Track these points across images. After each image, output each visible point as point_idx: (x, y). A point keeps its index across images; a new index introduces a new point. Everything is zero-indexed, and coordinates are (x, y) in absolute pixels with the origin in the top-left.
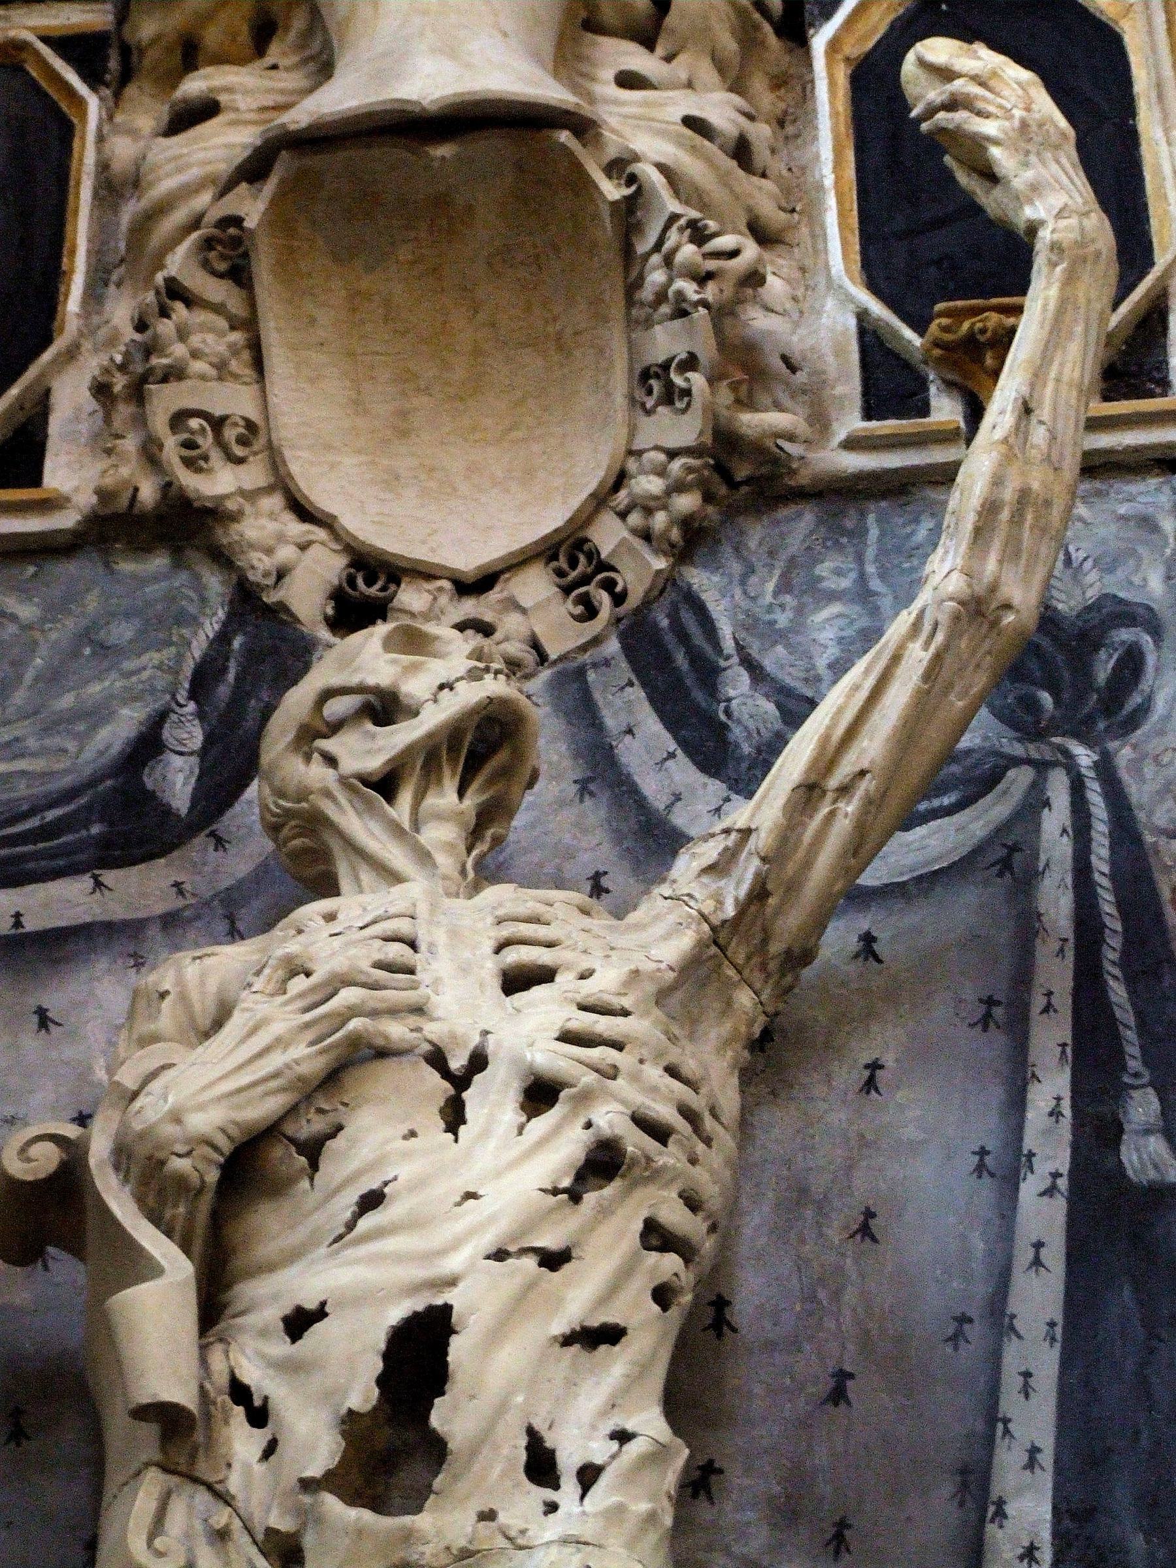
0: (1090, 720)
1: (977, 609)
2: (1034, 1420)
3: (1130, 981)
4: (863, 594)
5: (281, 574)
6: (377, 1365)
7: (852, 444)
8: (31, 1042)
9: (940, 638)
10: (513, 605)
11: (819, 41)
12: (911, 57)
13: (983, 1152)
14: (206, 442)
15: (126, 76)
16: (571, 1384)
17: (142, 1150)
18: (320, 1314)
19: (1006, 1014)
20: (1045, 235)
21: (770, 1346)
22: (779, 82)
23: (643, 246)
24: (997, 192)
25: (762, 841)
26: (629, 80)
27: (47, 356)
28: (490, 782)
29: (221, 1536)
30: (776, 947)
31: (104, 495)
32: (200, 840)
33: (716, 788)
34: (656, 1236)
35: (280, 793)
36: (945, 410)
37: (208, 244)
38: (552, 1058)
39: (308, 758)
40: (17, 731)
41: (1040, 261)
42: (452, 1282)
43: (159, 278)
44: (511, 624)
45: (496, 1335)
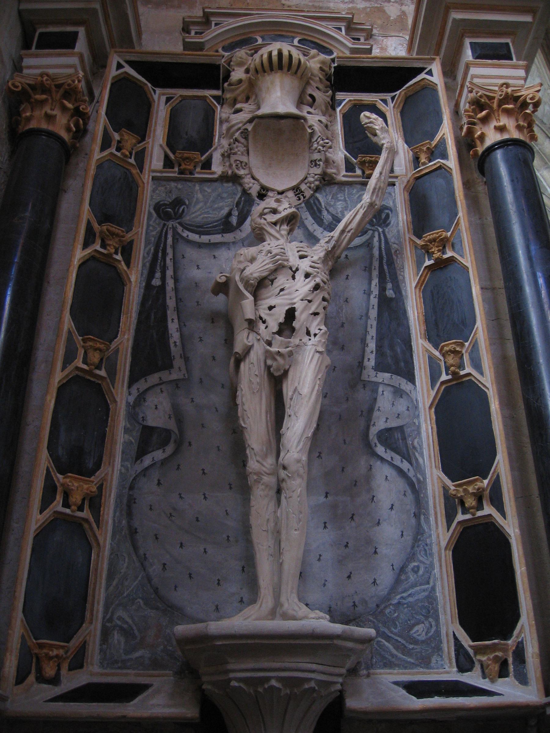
0: (381, 224)
1: (371, 205)
2: (373, 332)
3: (388, 265)
4: (345, 200)
5: (250, 188)
6: (284, 316)
7: (344, 176)
8: (213, 261)
9: (365, 209)
10: (286, 197)
11: (338, 110)
12: (362, 114)
13: (365, 290)
14: (239, 165)
16: (312, 321)
17: (246, 279)
18: (274, 307)
19: (368, 269)
20: (385, 146)
21: (332, 318)
22: (330, 116)
23: (313, 141)
24: (376, 138)
25: (335, 238)
28: (292, 225)
29: (259, 340)
30: (336, 256)
31: (223, 172)
32: (238, 230)
33: (321, 229)
34: (324, 299)
35: (256, 224)
36: (359, 172)
37: (242, 133)
38: (310, 270)
39: (261, 219)
41: (384, 150)
42: (295, 304)
43: (234, 137)
45: (302, 312)
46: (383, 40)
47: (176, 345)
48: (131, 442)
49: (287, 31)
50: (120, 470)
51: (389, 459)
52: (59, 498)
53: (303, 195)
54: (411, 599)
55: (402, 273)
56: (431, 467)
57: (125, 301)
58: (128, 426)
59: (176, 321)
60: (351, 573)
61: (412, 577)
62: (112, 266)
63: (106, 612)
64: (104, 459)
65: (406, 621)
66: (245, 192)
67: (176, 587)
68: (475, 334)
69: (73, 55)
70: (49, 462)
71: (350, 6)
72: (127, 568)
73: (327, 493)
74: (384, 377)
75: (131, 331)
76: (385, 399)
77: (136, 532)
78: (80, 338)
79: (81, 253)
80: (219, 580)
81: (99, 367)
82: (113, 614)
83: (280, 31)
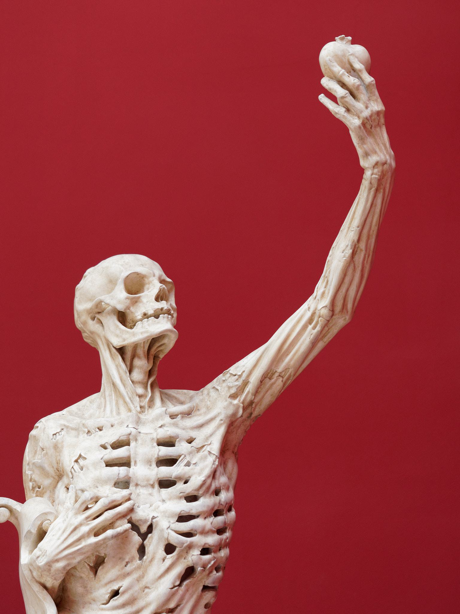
9: (318, 328)
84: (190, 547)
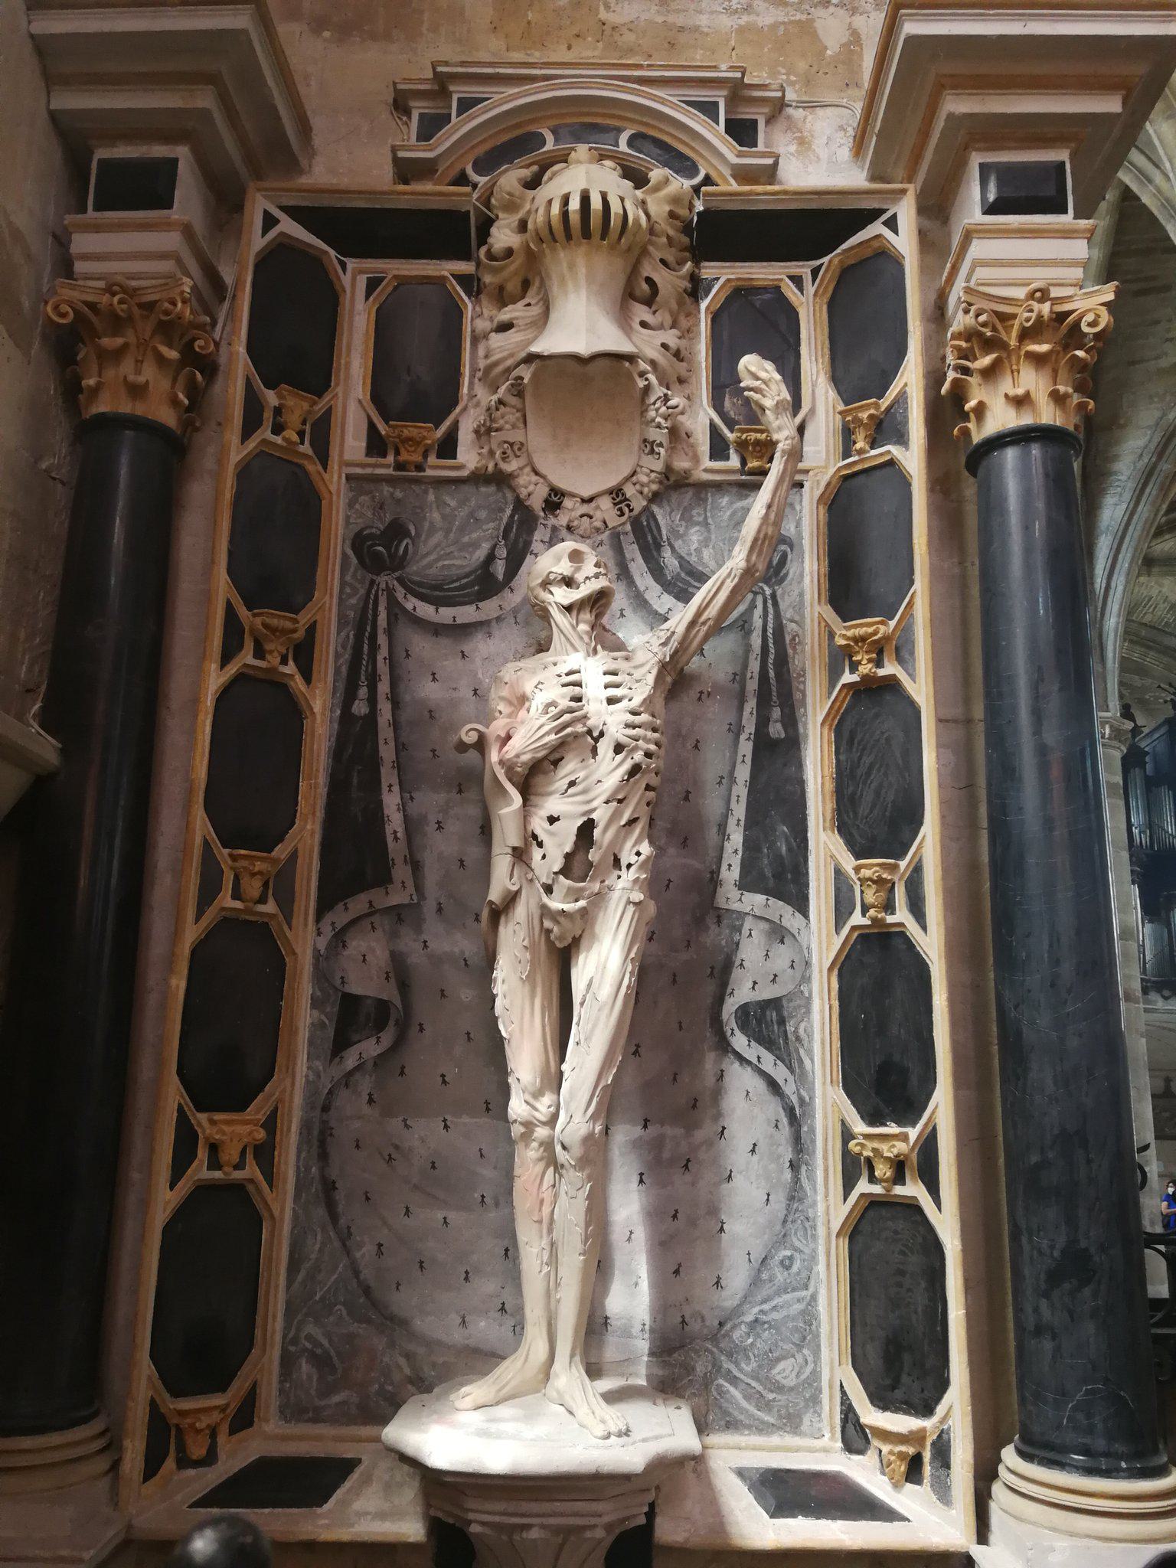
0: (770, 579)
2: (739, 811)
8: (460, 663)
9: (736, 580)
10: (598, 507)
11: (704, 305)
14: (509, 452)
15: (479, 292)
18: (558, 819)
20: (780, 446)
25: (677, 637)
26: (644, 324)
27: (458, 409)
29: (531, 880)
33: (658, 588)
34: (648, 788)
36: (734, 462)
40: (452, 549)
41: (777, 455)
42: (594, 810)
44: (598, 515)
46: (805, 118)
47: (396, 839)
48: (322, 1025)
49: (604, 115)
50: (307, 1076)
51: (755, 1061)
52: (202, 1154)
53: (628, 506)
54: (775, 1315)
55: (801, 687)
56: (824, 1083)
57: (305, 750)
58: (319, 993)
59: (396, 788)
60: (680, 1265)
61: (780, 1276)
62: (279, 687)
63: (287, 1328)
64: (278, 1059)
65: (766, 1353)
66: (520, 505)
67: (398, 1284)
68: (920, 847)
69: (166, 226)
70: (182, 1096)
71: (745, 19)
72: (320, 1250)
73: (646, 1121)
74: (755, 901)
75: (318, 814)
76: (751, 950)
77: (335, 1188)
78: (226, 851)
79: (218, 677)
80: (467, 1273)
81: (262, 900)
82: (298, 1330)
83: (588, 122)
84: (635, 749)
